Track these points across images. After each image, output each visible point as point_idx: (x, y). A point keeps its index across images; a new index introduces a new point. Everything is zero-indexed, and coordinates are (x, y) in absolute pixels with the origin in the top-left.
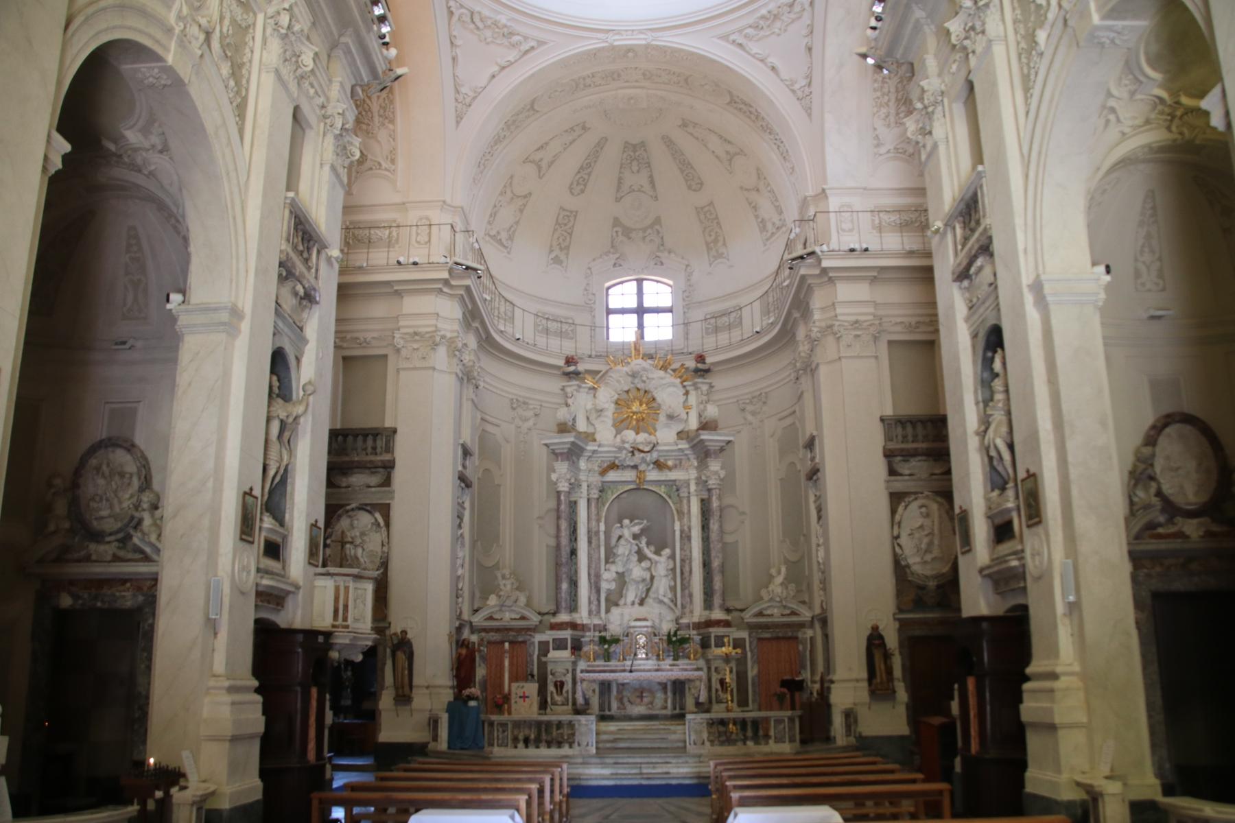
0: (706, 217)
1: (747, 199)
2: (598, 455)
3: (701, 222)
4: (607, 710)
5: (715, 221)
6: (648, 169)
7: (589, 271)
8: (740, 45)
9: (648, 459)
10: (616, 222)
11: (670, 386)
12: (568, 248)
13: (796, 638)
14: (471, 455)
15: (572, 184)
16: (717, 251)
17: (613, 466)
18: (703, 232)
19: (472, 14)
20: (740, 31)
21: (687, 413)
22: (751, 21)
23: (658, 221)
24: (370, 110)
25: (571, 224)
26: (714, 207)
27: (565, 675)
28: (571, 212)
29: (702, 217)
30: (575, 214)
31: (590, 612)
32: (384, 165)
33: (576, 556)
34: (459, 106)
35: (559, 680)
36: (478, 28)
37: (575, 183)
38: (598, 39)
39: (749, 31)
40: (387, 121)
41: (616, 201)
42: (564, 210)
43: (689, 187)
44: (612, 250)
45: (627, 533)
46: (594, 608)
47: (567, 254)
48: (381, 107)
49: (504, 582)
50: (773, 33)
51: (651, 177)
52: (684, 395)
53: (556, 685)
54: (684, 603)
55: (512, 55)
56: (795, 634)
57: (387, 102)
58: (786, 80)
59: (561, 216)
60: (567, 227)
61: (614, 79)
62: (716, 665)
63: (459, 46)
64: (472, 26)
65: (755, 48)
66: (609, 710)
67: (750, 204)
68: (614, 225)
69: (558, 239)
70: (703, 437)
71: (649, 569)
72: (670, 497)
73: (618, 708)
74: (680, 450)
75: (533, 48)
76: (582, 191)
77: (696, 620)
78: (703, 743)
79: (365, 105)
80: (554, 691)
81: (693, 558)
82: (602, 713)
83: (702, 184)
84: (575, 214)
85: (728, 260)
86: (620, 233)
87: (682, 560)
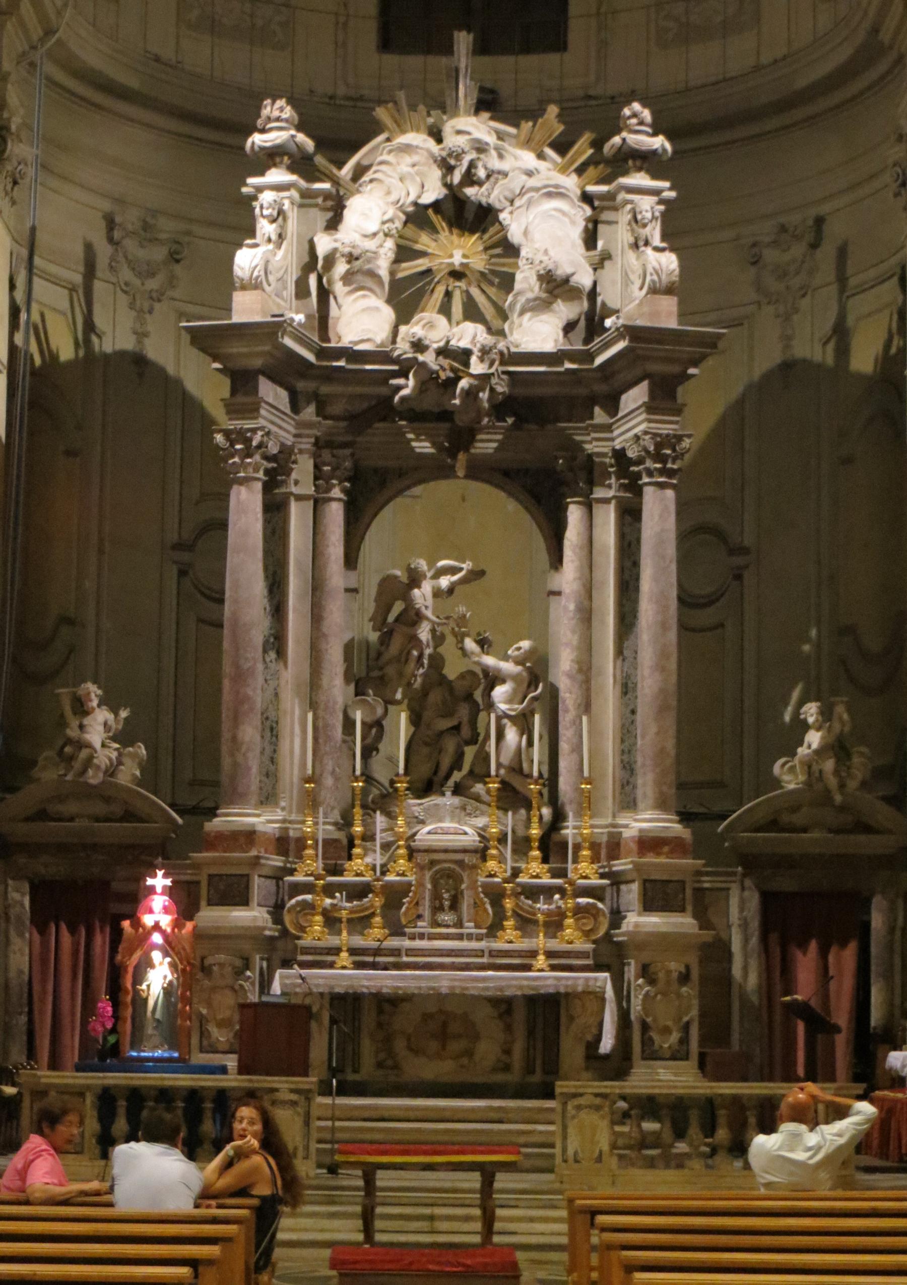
11: (549, 195)
66: (356, 1071)
73: (380, 1065)
78: (599, 1159)
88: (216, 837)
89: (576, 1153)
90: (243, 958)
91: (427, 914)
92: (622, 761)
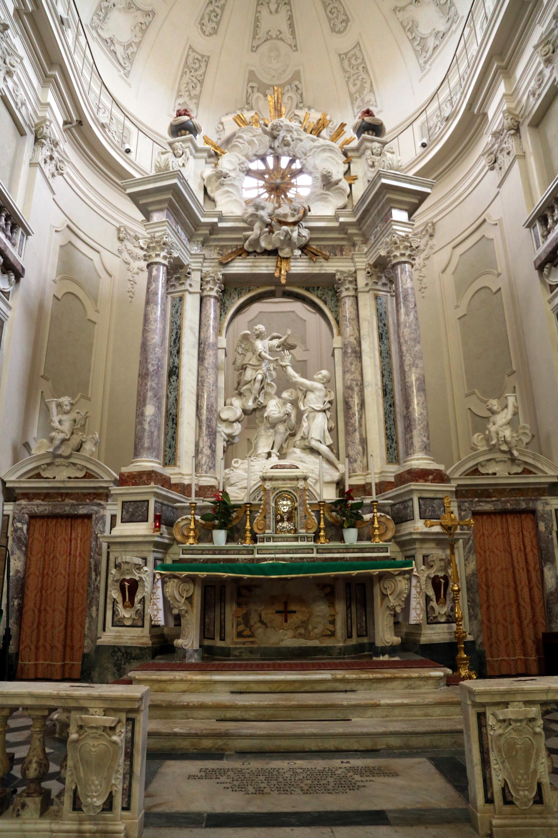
0: (350, 64)
1: (401, 23)
2: (220, 236)
3: (345, 71)
4: (217, 638)
5: (360, 68)
6: (288, 8)
7: (221, 127)
9: (295, 235)
10: (252, 76)
11: (324, 150)
12: (198, 97)
13: (533, 512)
14: (27, 233)
15: (202, 19)
16: (362, 100)
17: (242, 252)
18: (347, 82)
21: (350, 186)
23: (297, 76)
25: (200, 72)
26: (360, 50)
27: (139, 568)
28: (203, 56)
29: (346, 62)
30: (204, 60)
31: (197, 467)
33: (178, 376)
35: (128, 577)
37: (207, 18)
41: (252, 51)
42: (194, 51)
43: (333, 30)
44: (247, 106)
45: (261, 345)
46: (204, 460)
47: (197, 104)
49: (60, 417)
51: (291, 18)
52: (344, 163)
53: (122, 589)
54: (351, 453)
56: (531, 505)
59: (190, 59)
60: (197, 73)
62: (425, 552)
66: (222, 639)
67: (404, 28)
68: (249, 82)
69: (188, 84)
70: (384, 181)
71: (295, 403)
72: (325, 303)
73: (240, 635)
74: (343, 227)
76: (215, 31)
77: (374, 479)
78: (539, 799)
80: (120, 600)
81: (365, 383)
82: (207, 643)
83: (346, 21)
84: (204, 60)
85: (376, 106)
86: (255, 90)
87: (347, 388)
88: (128, 476)
89: (505, 789)
90: (143, 559)
91: (272, 524)
92: (386, 434)
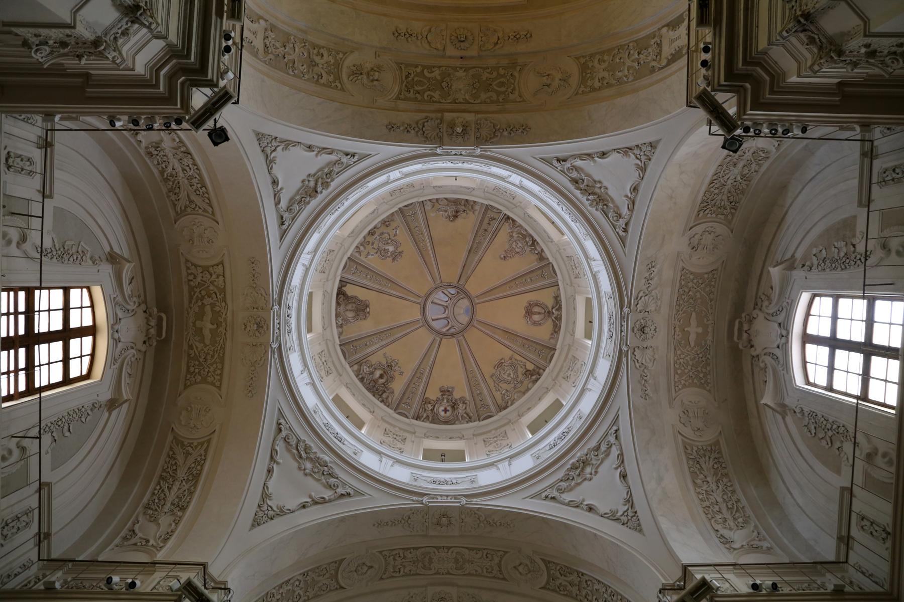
8: (553, 498)
19: (299, 441)
20: (551, 487)
22: (561, 474)
24: (164, 499)
32: (152, 542)
34: (261, 514)
36: (301, 457)
38: (413, 500)
39: (564, 485)
40: (178, 509)
48: (177, 497)
50: (585, 479)
55: (328, 494)
57: (186, 493)
58: (605, 514)
61: (424, 567)
63: (278, 463)
64: (295, 451)
65: (567, 497)
75: (349, 494)
79: (162, 495)
